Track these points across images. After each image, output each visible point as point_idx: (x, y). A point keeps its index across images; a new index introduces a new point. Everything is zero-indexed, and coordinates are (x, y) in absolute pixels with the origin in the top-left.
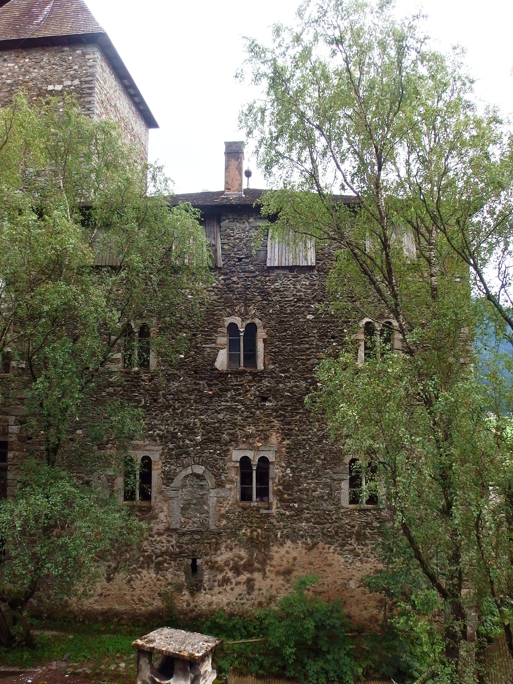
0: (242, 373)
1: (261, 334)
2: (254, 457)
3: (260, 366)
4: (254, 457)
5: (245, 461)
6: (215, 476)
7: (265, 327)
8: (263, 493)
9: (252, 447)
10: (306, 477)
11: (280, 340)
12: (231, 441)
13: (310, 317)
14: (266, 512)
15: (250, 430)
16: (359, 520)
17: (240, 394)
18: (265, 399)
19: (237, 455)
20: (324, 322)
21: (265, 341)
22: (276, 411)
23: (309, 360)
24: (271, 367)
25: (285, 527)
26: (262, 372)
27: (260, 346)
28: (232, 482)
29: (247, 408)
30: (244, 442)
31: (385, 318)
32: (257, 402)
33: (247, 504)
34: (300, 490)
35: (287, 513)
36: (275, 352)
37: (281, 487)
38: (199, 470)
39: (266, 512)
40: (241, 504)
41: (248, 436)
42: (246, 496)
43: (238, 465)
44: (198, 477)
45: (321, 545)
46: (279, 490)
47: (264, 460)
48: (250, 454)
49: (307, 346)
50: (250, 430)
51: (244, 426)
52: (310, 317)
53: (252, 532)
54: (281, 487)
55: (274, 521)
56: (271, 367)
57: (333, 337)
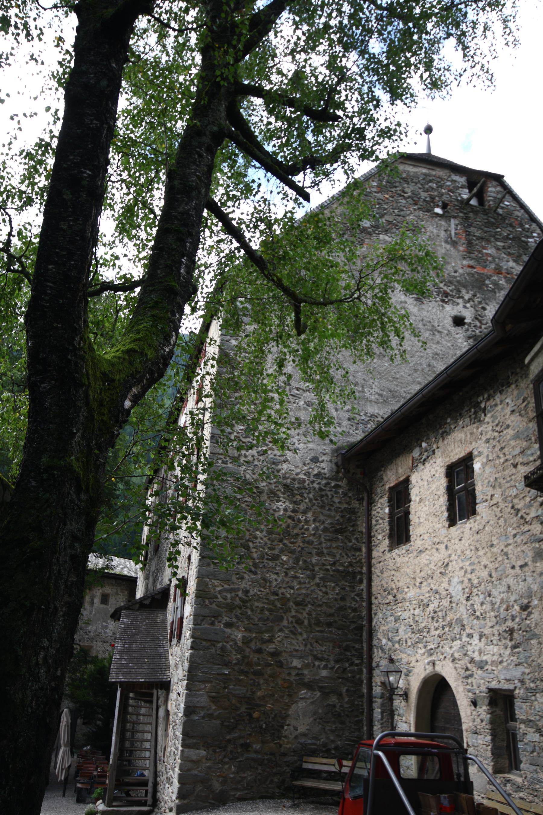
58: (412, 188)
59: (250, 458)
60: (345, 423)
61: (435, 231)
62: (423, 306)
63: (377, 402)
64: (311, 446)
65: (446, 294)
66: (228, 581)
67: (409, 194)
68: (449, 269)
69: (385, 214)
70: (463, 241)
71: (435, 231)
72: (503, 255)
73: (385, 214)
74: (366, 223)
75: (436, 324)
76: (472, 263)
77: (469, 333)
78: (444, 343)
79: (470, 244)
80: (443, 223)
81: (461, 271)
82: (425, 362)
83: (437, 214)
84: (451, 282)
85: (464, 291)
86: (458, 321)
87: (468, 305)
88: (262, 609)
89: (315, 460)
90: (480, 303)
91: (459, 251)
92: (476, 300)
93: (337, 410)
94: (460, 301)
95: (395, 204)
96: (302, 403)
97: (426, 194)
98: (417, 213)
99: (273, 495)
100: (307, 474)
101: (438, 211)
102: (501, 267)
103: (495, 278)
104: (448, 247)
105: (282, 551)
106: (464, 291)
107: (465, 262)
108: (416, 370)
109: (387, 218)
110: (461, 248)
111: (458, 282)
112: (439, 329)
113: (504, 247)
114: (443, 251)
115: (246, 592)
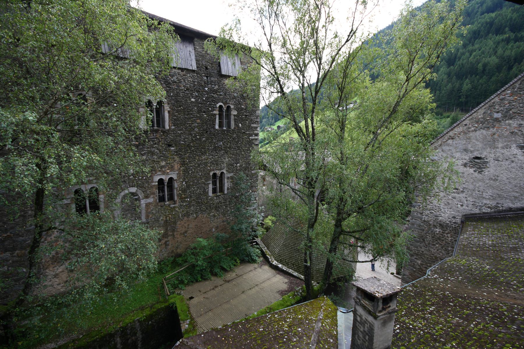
0: (157, 131)
1: (167, 108)
2: (166, 178)
3: (167, 127)
4: (166, 178)
5: (161, 181)
6: (143, 192)
7: (168, 104)
8: (171, 198)
9: (164, 173)
10: (193, 185)
11: (177, 111)
12: (152, 170)
13: (193, 100)
14: (173, 206)
15: (163, 163)
16: (216, 201)
17: (155, 144)
18: (170, 146)
19: (157, 178)
20: (200, 103)
21: (169, 112)
22: (176, 152)
23: (192, 124)
24: (173, 127)
25: (183, 211)
26: (168, 130)
27: (167, 115)
28: (153, 194)
29: (160, 151)
30: (160, 171)
31: (227, 104)
32: (166, 147)
33: (162, 203)
34: (190, 192)
35: (184, 204)
36: (175, 119)
37: (180, 192)
38: (133, 190)
39: (173, 206)
40: (159, 204)
41: (162, 167)
42: (162, 199)
43: (157, 184)
44: (133, 194)
45: (200, 216)
46: (180, 193)
47: (171, 179)
48: (163, 177)
49: (192, 116)
50: (163, 163)
51: (159, 162)
52: (193, 100)
53: (166, 218)
54: (180, 192)
55: (177, 209)
56: (173, 127)
57: (204, 112)
63: (489, 199)
64: (453, 213)
66: (417, 248)
69: (513, 108)
73: (513, 108)
74: (499, 116)
88: (428, 258)
89: (454, 217)
93: (467, 201)
96: (450, 197)
99: (435, 226)
100: (450, 222)
105: (437, 244)
108: (515, 186)
109: (513, 110)
115: (423, 252)
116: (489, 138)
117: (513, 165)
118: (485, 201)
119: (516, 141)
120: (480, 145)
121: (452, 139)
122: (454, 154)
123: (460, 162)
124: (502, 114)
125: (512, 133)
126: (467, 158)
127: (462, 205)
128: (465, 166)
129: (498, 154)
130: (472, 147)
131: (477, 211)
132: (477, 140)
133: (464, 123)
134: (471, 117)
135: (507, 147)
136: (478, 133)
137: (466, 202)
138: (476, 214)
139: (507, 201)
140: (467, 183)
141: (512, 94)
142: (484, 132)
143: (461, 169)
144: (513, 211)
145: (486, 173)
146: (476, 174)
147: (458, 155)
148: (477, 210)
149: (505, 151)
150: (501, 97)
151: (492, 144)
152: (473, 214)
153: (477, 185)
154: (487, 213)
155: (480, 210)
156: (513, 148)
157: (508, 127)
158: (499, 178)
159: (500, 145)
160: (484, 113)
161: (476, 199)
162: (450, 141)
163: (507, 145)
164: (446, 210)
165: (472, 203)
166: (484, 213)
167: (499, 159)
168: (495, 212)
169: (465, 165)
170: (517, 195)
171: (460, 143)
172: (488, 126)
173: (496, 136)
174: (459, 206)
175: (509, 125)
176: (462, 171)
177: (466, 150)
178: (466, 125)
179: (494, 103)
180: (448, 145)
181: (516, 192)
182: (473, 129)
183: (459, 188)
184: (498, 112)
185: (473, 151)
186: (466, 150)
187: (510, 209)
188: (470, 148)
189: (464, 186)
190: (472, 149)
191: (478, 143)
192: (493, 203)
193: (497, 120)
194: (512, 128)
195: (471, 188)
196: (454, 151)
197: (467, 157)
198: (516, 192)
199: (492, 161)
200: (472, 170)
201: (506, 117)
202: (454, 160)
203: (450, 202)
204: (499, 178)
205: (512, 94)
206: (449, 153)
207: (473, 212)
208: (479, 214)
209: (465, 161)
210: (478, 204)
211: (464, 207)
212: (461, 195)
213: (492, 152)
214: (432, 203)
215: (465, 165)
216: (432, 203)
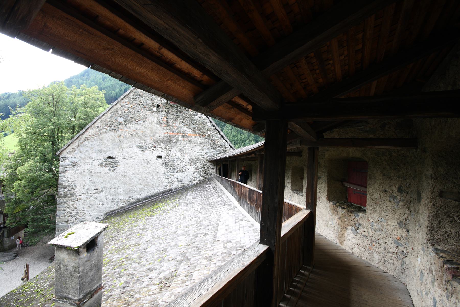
58: (144, 100)
59: (72, 221)
60: (110, 203)
61: (152, 119)
62: (144, 153)
63: (123, 194)
64: (96, 213)
65: (155, 147)
67: (143, 103)
68: (157, 135)
70: (165, 122)
71: (152, 119)
72: (182, 126)
75: (149, 160)
76: (167, 131)
77: (163, 162)
78: (152, 167)
79: (168, 122)
80: (156, 115)
81: (162, 136)
82: (143, 176)
83: (154, 111)
84: (157, 141)
85: (162, 144)
86: (160, 157)
87: (163, 150)
90: (169, 148)
91: (162, 127)
92: (167, 148)
94: (160, 149)
95: (135, 109)
96: (92, 198)
97: (150, 102)
98: (145, 112)
101: (155, 109)
102: (181, 131)
103: (177, 136)
104: (157, 125)
106: (162, 144)
107: (165, 131)
109: (131, 116)
110: (163, 125)
111: (160, 141)
112: (150, 162)
113: (183, 122)
114: (155, 128)
116: (117, 139)
117: (136, 161)
118: (120, 197)
119: (135, 142)
120: (111, 146)
121: (88, 140)
122: (91, 155)
123: (97, 163)
124: (124, 119)
125: (132, 135)
126: (102, 158)
127: (103, 204)
128: (101, 166)
129: (125, 154)
130: (104, 148)
131: (115, 207)
132: (108, 141)
133: (96, 125)
134: (101, 120)
135: (130, 147)
136: (108, 134)
137: (105, 201)
138: (115, 210)
139: (136, 193)
140: (105, 182)
141: (129, 103)
142: (112, 133)
143: (99, 169)
144: (140, 201)
145: (118, 171)
146: (111, 172)
147: (94, 156)
148: (116, 206)
149: (129, 150)
150: (122, 104)
151: (119, 145)
152: (112, 211)
153: (113, 183)
154: (123, 207)
155: (117, 205)
156: (134, 148)
157: (129, 130)
158: (128, 174)
159: (125, 145)
160: (111, 117)
161: (113, 196)
162: (86, 142)
163: (130, 145)
164: (90, 212)
165: (111, 201)
166: (121, 208)
167: (126, 158)
168: (128, 205)
169: (101, 165)
170: (141, 187)
171: (94, 144)
172: (115, 128)
173: (121, 138)
174: (101, 205)
175: (129, 128)
176: (99, 171)
177: (100, 151)
178: (98, 127)
179: (117, 108)
180: (85, 146)
181: (141, 184)
182: (104, 130)
183: (99, 188)
184: (121, 117)
185: (106, 151)
186: (100, 151)
187: (139, 201)
188: (103, 149)
189: (103, 185)
190: (105, 150)
191: (109, 144)
192: (125, 197)
193: (120, 123)
194: (132, 131)
195: (108, 187)
196: (90, 151)
197: (102, 157)
198: (141, 184)
199: (121, 160)
200: (107, 169)
201: (127, 121)
202: (91, 161)
203: (92, 203)
204: (128, 174)
205: (129, 103)
206: (86, 154)
207: (112, 209)
208: (117, 209)
209: (101, 161)
210: (115, 201)
211: (105, 206)
212: (102, 195)
213: (120, 151)
214: (76, 208)
215: (101, 165)
216: (76, 208)
